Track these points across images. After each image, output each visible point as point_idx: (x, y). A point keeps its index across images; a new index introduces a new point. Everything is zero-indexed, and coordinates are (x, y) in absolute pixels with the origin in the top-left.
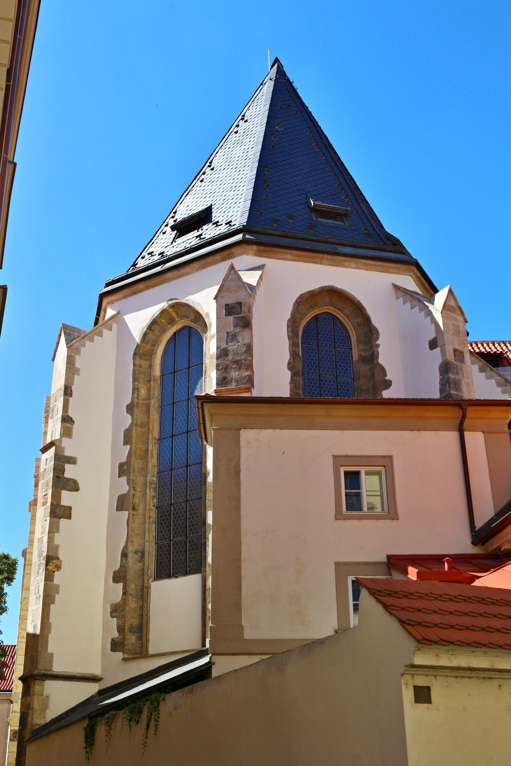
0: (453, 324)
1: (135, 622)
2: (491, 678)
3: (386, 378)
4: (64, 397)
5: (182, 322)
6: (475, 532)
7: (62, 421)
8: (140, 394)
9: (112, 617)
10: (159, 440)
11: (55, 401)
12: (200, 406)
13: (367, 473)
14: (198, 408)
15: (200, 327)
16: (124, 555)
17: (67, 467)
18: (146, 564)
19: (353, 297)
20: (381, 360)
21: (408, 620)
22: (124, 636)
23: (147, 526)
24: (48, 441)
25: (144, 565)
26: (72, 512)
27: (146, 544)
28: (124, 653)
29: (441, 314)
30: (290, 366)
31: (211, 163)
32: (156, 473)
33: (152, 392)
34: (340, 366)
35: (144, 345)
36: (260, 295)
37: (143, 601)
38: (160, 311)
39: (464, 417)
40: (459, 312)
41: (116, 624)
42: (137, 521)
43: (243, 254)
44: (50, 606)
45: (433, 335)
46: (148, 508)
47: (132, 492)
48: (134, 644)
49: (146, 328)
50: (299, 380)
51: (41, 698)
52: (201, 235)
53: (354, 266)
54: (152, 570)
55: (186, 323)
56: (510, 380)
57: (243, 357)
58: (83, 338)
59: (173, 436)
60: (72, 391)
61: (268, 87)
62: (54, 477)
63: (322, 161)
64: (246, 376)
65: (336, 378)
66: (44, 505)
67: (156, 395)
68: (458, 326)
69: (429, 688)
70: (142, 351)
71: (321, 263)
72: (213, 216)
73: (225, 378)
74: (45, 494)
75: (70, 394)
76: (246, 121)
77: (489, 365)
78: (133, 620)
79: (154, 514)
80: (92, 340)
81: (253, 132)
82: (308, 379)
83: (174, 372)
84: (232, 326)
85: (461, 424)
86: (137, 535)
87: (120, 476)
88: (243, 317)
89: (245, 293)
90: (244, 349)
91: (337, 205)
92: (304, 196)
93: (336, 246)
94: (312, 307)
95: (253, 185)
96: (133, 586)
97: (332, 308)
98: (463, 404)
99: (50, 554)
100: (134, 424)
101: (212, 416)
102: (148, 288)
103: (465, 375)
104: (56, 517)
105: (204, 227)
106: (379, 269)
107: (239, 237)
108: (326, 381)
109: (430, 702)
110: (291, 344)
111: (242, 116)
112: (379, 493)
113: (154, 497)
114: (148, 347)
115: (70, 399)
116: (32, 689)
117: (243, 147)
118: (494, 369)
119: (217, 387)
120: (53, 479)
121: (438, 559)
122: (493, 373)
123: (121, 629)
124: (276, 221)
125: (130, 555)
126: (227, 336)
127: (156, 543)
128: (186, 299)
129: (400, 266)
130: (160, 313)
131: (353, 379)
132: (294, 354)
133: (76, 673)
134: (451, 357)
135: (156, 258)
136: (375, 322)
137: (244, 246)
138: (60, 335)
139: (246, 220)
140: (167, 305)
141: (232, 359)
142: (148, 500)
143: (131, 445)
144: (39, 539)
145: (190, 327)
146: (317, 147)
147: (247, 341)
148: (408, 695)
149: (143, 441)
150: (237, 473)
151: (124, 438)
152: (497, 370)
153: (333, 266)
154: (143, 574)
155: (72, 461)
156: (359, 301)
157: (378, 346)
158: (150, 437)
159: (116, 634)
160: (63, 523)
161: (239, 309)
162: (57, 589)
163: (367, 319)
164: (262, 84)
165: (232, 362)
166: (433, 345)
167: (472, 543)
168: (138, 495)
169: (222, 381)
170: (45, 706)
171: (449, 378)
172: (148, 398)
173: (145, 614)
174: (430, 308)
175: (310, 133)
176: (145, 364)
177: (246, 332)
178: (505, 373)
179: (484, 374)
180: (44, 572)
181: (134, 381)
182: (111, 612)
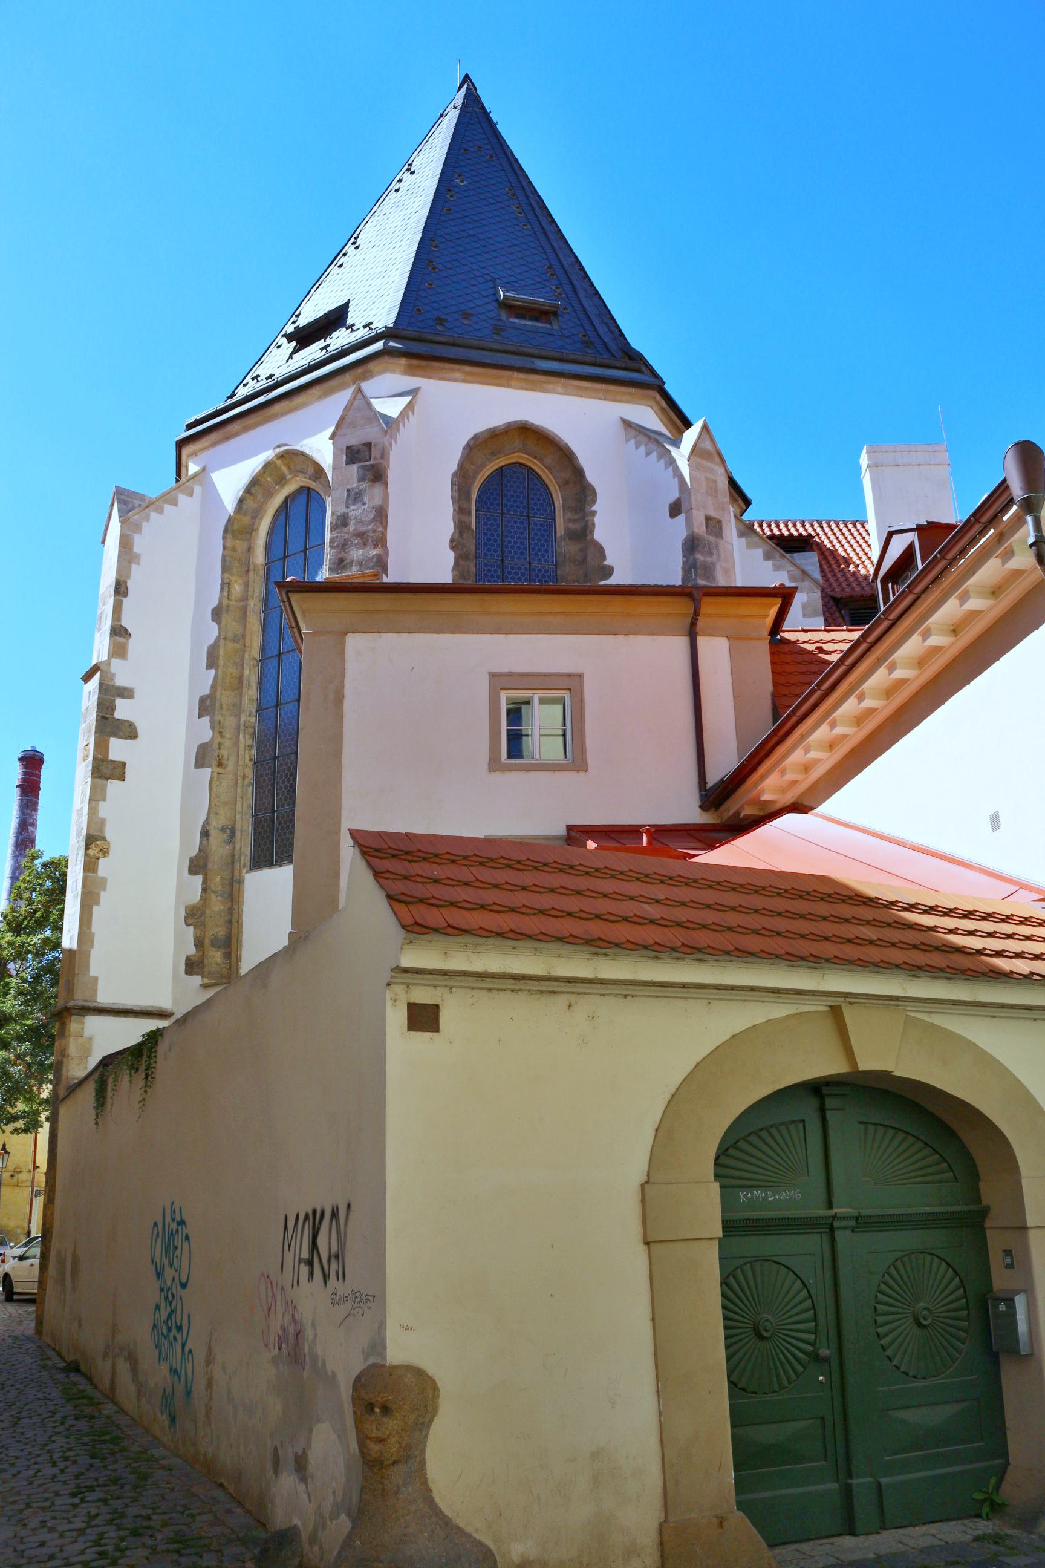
0: (707, 479)
1: (220, 932)
2: (554, 992)
3: (605, 563)
4: (115, 596)
5: (296, 481)
6: (706, 791)
7: (111, 634)
8: (233, 591)
9: (187, 925)
10: (260, 661)
11: (104, 605)
12: (285, 599)
13: (543, 701)
14: (283, 602)
15: (321, 486)
16: (205, 833)
17: (119, 702)
18: (238, 847)
19: (557, 439)
20: (599, 535)
21: (402, 894)
22: (204, 953)
23: (239, 790)
24: (94, 662)
25: (234, 848)
26: (127, 771)
27: (237, 817)
28: (203, 977)
29: (688, 461)
30: (454, 544)
31: (356, 238)
32: (254, 710)
33: (250, 589)
34: (536, 545)
35: (239, 517)
36: (406, 434)
37: (232, 901)
38: (263, 464)
39: (696, 613)
40: (717, 460)
41: (192, 935)
42: (225, 783)
43: (385, 371)
44: (92, 909)
45: (674, 495)
46: (241, 763)
47: (218, 739)
48: (218, 965)
49: (243, 490)
50: (469, 566)
51: (81, 1040)
52: (328, 346)
53: (560, 389)
54: (246, 856)
55: (302, 481)
56: (811, 573)
57: (370, 527)
58: (147, 507)
59: (280, 654)
60: (127, 589)
61: (450, 120)
62: (99, 718)
63: (525, 232)
64: (373, 556)
65: (530, 563)
66: (84, 760)
67: (257, 592)
68: (716, 482)
69: (437, 1006)
70: (236, 527)
71: (509, 386)
72: (349, 317)
73: (342, 560)
74: (86, 743)
75: (124, 592)
76: (413, 173)
77: (778, 549)
78: (217, 930)
79: (250, 773)
80: (160, 511)
81: (421, 189)
82: (485, 565)
83: (285, 557)
84: (356, 480)
85: (693, 624)
86: (225, 804)
87: (200, 716)
88: (372, 466)
89: (376, 429)
90: (372, 515)
91: (541, 298)
92: (491, 284)
93: (534, 359)
94: (494, 454)
95: (409, 268)
96: (218, 879)
97: (526, 456)
98: (696, 594)
99: (93, 832)
100: (222, 637)
101: (303, 612)
102: (246, 429)
103: (722, 555)
104: (100, 777)
105: (334, 334)
106: (601, 395)
107: (379, 345)
108: (513, 568)
109: (437, 1029)
110: (457, 509)
111: (409, 165)
112: (560, 732)
113: (252, 746)
114: (246, 520)
115: (124, 599)
116: (67, 1027)
117: (404, 212)
118: (788, 555)
119: (329, 574)
120: (97, 721)
121: (634, 831)
122: (784, 562)
123: (199, 943)
124: (441, 321)
125: (213, 833)
126: (348, 496)
127: (253, 816)
128: (301, 444)
129: (633, 390)
130: (262, 468)
131: (556, 565)
132: (461, 527)
133: (133, 1006)
134: (700, 529)
135: (263, 383)
136: (591, 476)
137: (386, 359)
138: (112, 505)
139: (393, 320)
140: (273, 455)
141: (354, 530)
142: (241, 752)
143: (217, 669)
144: (78, 811)
145: (309, 489)
146: (520, 210)
147: (377, 502)
148: (396, 1017)
149: (235, 663)
150: (339, 699)
151: (207, 659)
152: (791, 557)
153: (527, 389)
154: (233, 862)
155: (126, 693)
156: (567, 444)
157: (594, 513)
158: (246, 656)
159: (192, 950)
160: (113, 786)
161: (367, 453)
162: (103, 883)
163: (578, 473)
164: (441, 116)
165: (354, 535)
166: (675, 509)
167: (701, 807)
168: (227, 743)
169: (340, 564)
170: (87, 1052)
171: (695, 560)
172: (245, 598)
173: (234, 920)
174: (673, 453)
175: (509, 189)
176: (241, 546)
177: (377, 490)
178: (804, 562)
179: (770, 563)
180: (83, 859)
181: (223, 572)
182: (185, 917)
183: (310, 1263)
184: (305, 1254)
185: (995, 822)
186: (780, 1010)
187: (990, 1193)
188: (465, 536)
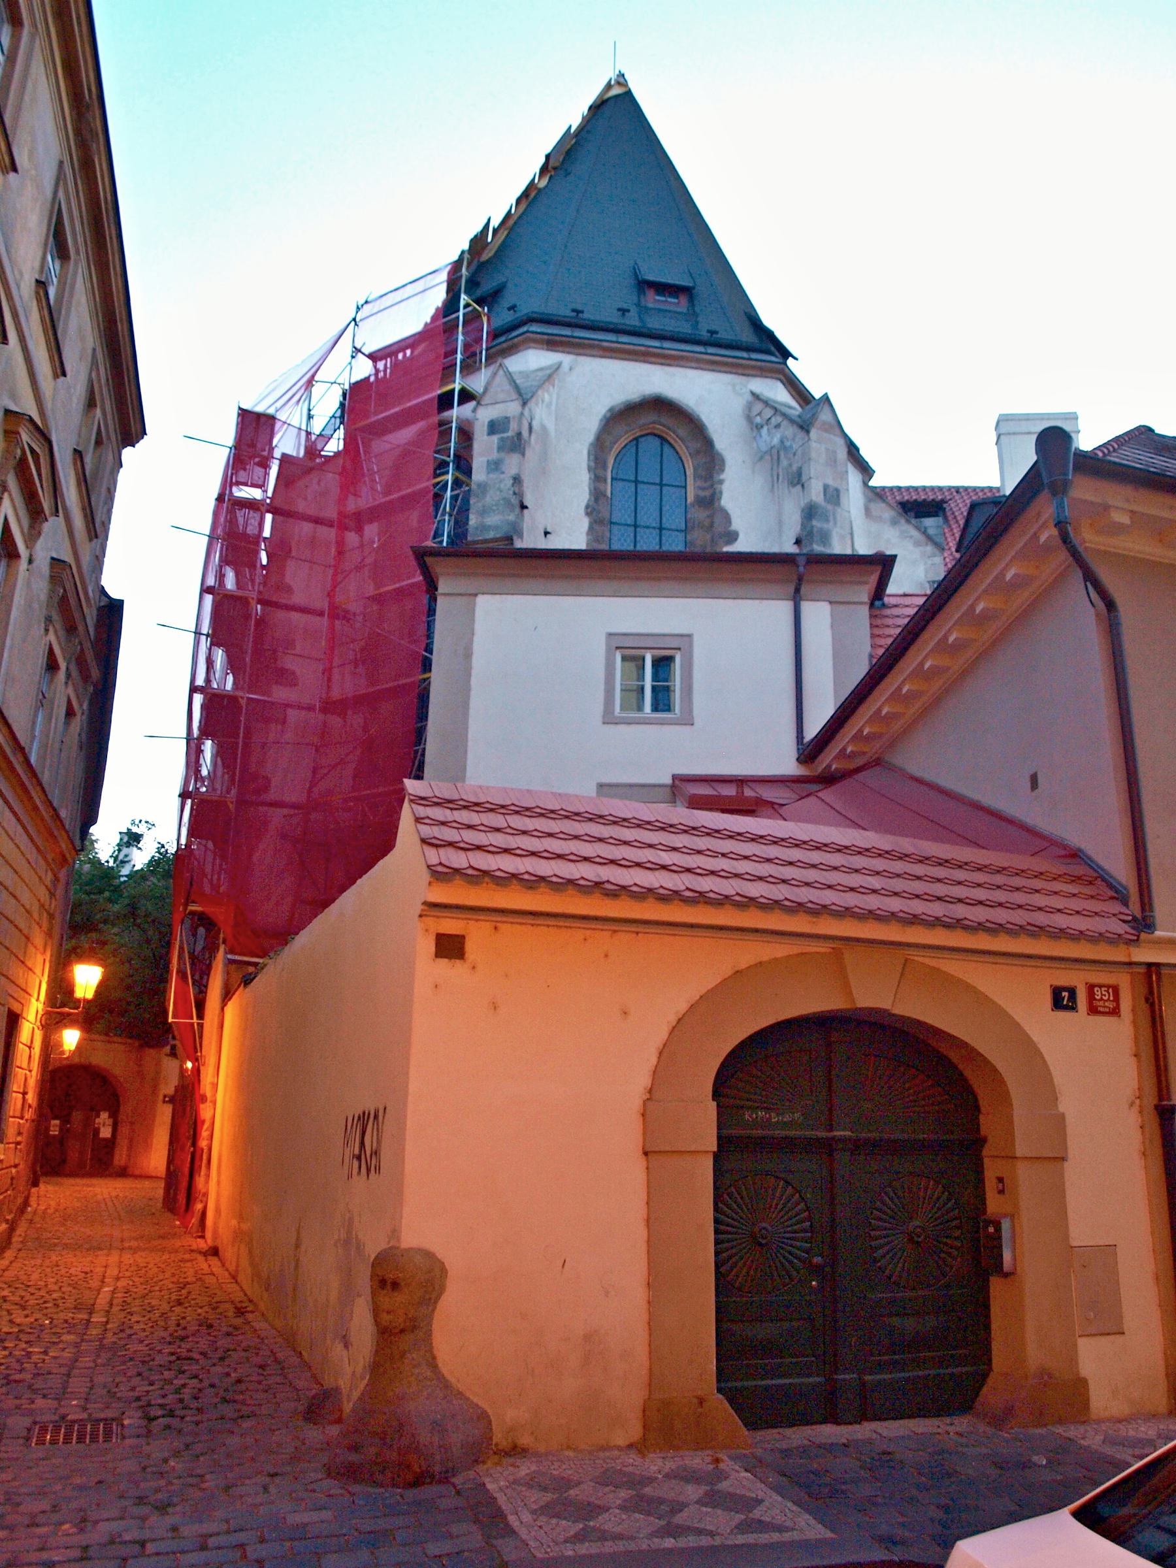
0: (827, 449)
20: (727, 501)
68: (835, 452)
84: (495, 450)
103: (839, 524)
147: (513, 471)
148: (428, 946)
157: (721, 482)
163: (708, 443)
167: (797, 759)
171: (812, 527)
183: (359, 1158)
184: (357, 1152)
185: (1034, 782)
186: (781, 950)
187: (988, 1124)
188: (600, 502)
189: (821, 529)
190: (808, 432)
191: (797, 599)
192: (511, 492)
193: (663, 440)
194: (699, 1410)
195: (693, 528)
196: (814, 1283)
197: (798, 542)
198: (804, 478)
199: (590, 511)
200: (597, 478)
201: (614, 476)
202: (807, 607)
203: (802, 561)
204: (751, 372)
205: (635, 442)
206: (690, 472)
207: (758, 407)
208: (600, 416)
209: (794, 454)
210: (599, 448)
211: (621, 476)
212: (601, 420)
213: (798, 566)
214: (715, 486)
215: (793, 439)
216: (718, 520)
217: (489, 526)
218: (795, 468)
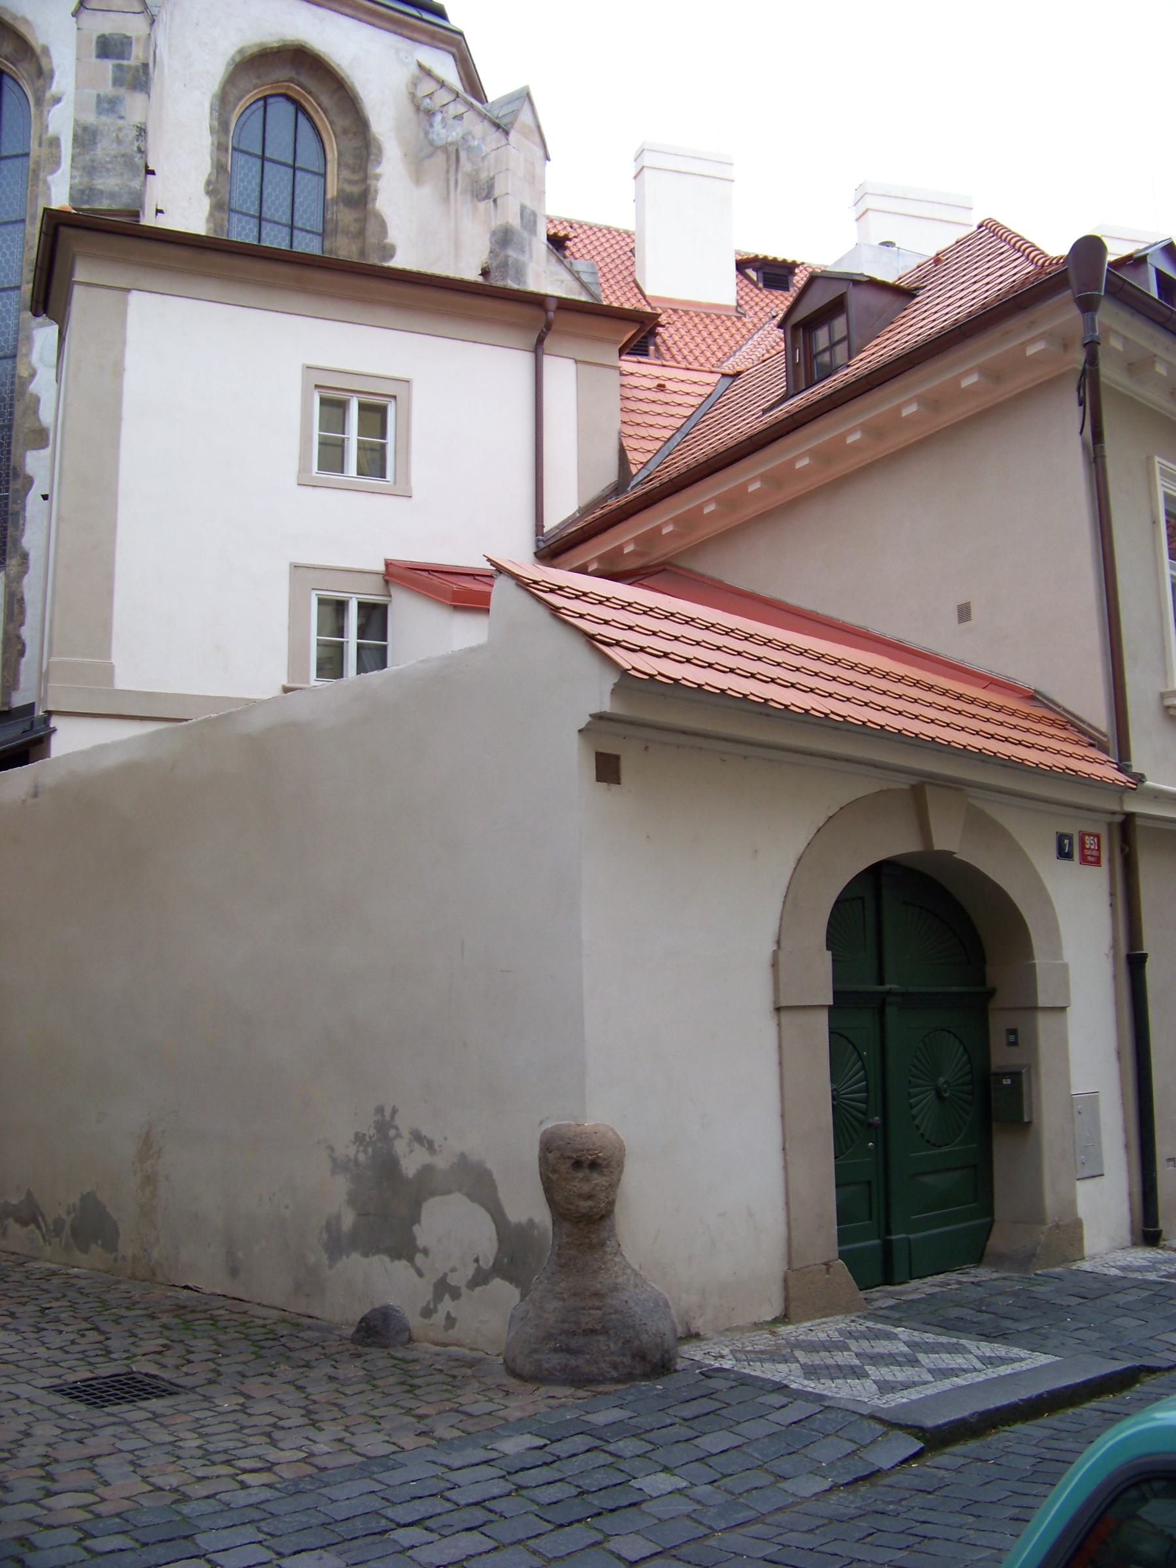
19: (341, 73)
30: (211, 188)
50: (223, 219)
134: (515, 221)
156: (352, 83)
157: (377, 177)
171: (507, 257)
185: (964, 613)
189: (517, 261)
190: (507, 133)
191: (538, 350)
192: (135, 149)
193: (299, 108)
194: (827, 1276)
195: (335, 232)
196: (870, 1144)
197: (485, 273)
198: (497, 192)
199: (212, 189)
200: (220, 147)
201: (236, 146)
202: (548, 362)
203: (552, 305)
204: (423, 38)
205: (261, 103)
206: (332, 155)
207: (427, 86)
208: (228, 57)
209: (483, 158)
210: (223, 101)
211: (243, 147)
212: (228, 64)
213: (546, 311)
214: (369, 182)
215: (483, 139)
216: (372, 227)
217: (102, 192)
218: (484, 176)
